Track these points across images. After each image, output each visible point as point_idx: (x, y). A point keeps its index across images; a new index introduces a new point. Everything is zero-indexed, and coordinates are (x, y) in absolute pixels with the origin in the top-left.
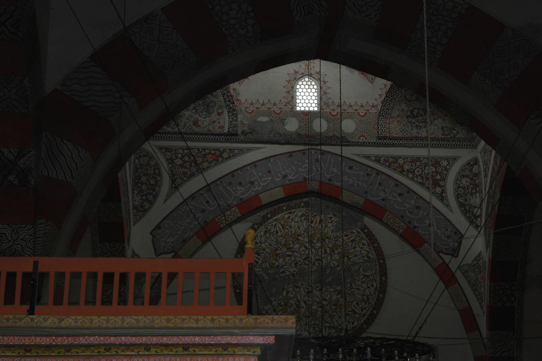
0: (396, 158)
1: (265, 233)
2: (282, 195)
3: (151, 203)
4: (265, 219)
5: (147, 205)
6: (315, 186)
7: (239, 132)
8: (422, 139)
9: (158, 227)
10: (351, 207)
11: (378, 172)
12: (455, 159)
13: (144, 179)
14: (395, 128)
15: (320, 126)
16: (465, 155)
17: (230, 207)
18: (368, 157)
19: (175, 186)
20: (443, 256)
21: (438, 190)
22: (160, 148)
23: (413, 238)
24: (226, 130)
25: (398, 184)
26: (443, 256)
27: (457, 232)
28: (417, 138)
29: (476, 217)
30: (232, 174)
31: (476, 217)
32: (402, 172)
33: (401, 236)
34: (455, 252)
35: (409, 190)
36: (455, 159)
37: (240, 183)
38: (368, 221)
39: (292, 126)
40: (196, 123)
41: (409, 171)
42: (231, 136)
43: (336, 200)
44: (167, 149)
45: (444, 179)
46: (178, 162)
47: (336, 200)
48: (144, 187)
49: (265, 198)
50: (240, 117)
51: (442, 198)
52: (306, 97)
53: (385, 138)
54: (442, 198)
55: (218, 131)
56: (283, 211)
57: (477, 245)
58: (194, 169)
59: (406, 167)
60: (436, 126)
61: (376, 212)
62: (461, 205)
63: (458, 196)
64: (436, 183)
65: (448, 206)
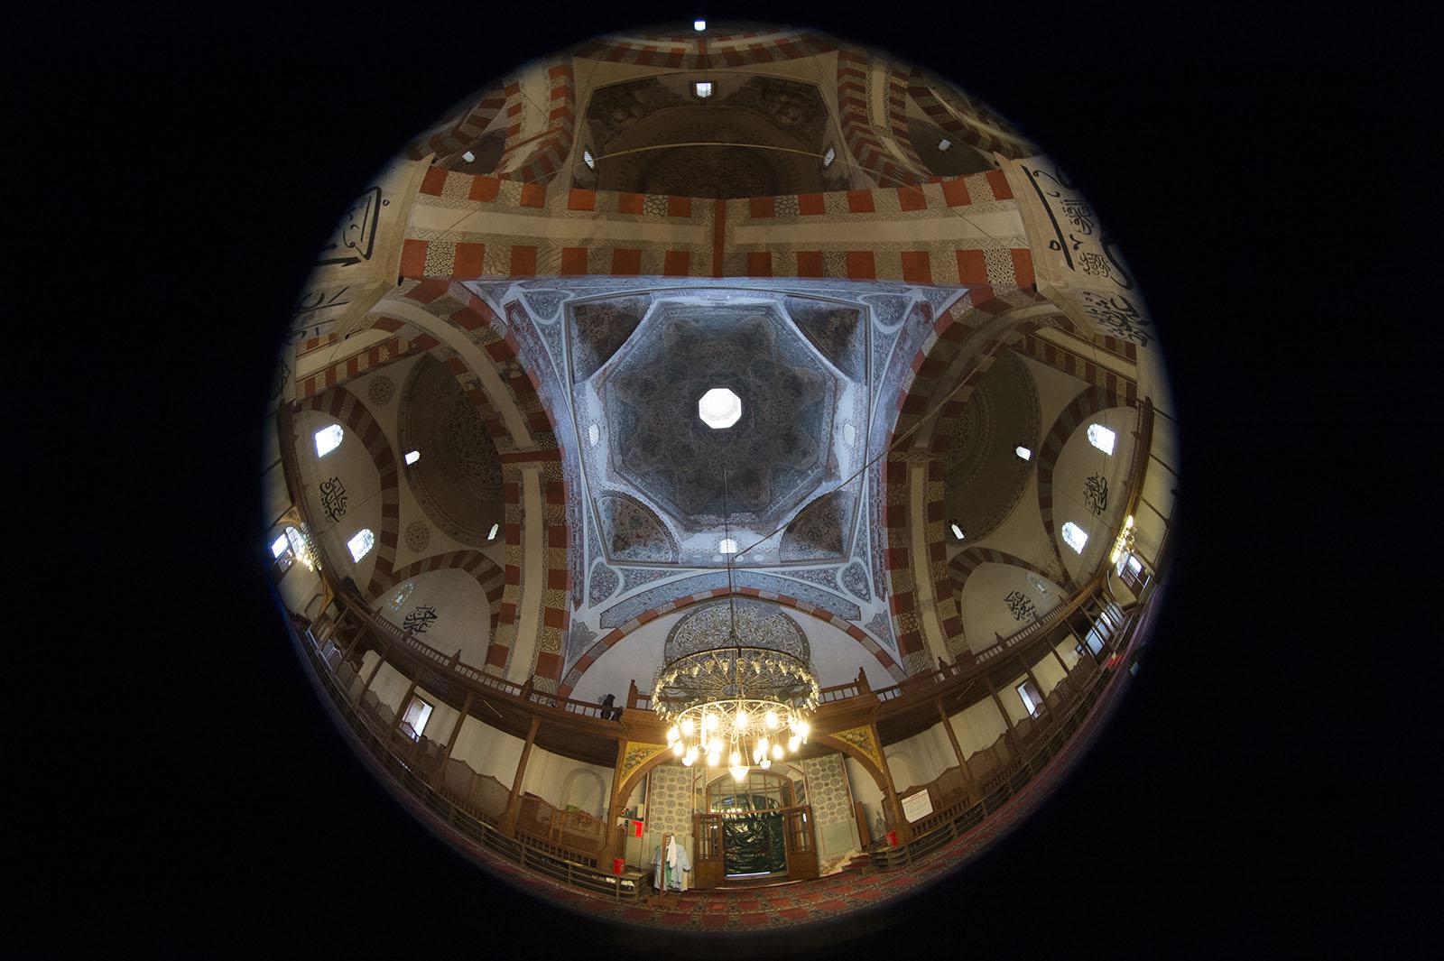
0: (797, 572)
1: (696, 621)
2: (712, 596)
3: (606, 597)
4: (696, 612)
5: (603, 597)
6: (739, 590)
7: (680, 562)
8: (812, 560)
9: (608, 611)
10: (769, 601)
11: (785, 580)
12: (837, 568)
13: (605, 584)
14: (792, 556)
15: (740, 559)
16: (843, 566)
17: (667, 602)
18: (776, 573)
19: (626, 589)
20: (852, 622)
21: (832, 585)
22: (622, 569)
23: (822, 615)
24: (670, 560)
25: (802, 585)
26: (852, 622)
27: (855, 605)
28: (808, 560)
29: (864, 596)
30: (671, 584)
31: (864, 596)
32: (803, 578)
33: (813, 615)
34: (858, 617)
35: (812, 587)
36: (837, 568)
37: (677, 589)
38: (783, 609)
39: (718, 559)
40: (649, 557)
41: (808, 577)
42: (674, 563)
43: (757, 597)
44: (626, 570)
45: (834, 579)
46: (632, 577)
47: (757, 597)
48: (604, 588)
49: (696, 598)
50: (681, 555)
51: (836, 588)
52: (728, 546)
53: (786, 561)
54: (836, 588)
55: (663, 560)
56: (712, 606)
57: (875, 608)
58: (643, 581)
59: (805, 575)
60: (819, 553)
61: (791, 603)
62: (851, 591)
63: (847, 587)
64: (829, 579)
65: (843, 592)
